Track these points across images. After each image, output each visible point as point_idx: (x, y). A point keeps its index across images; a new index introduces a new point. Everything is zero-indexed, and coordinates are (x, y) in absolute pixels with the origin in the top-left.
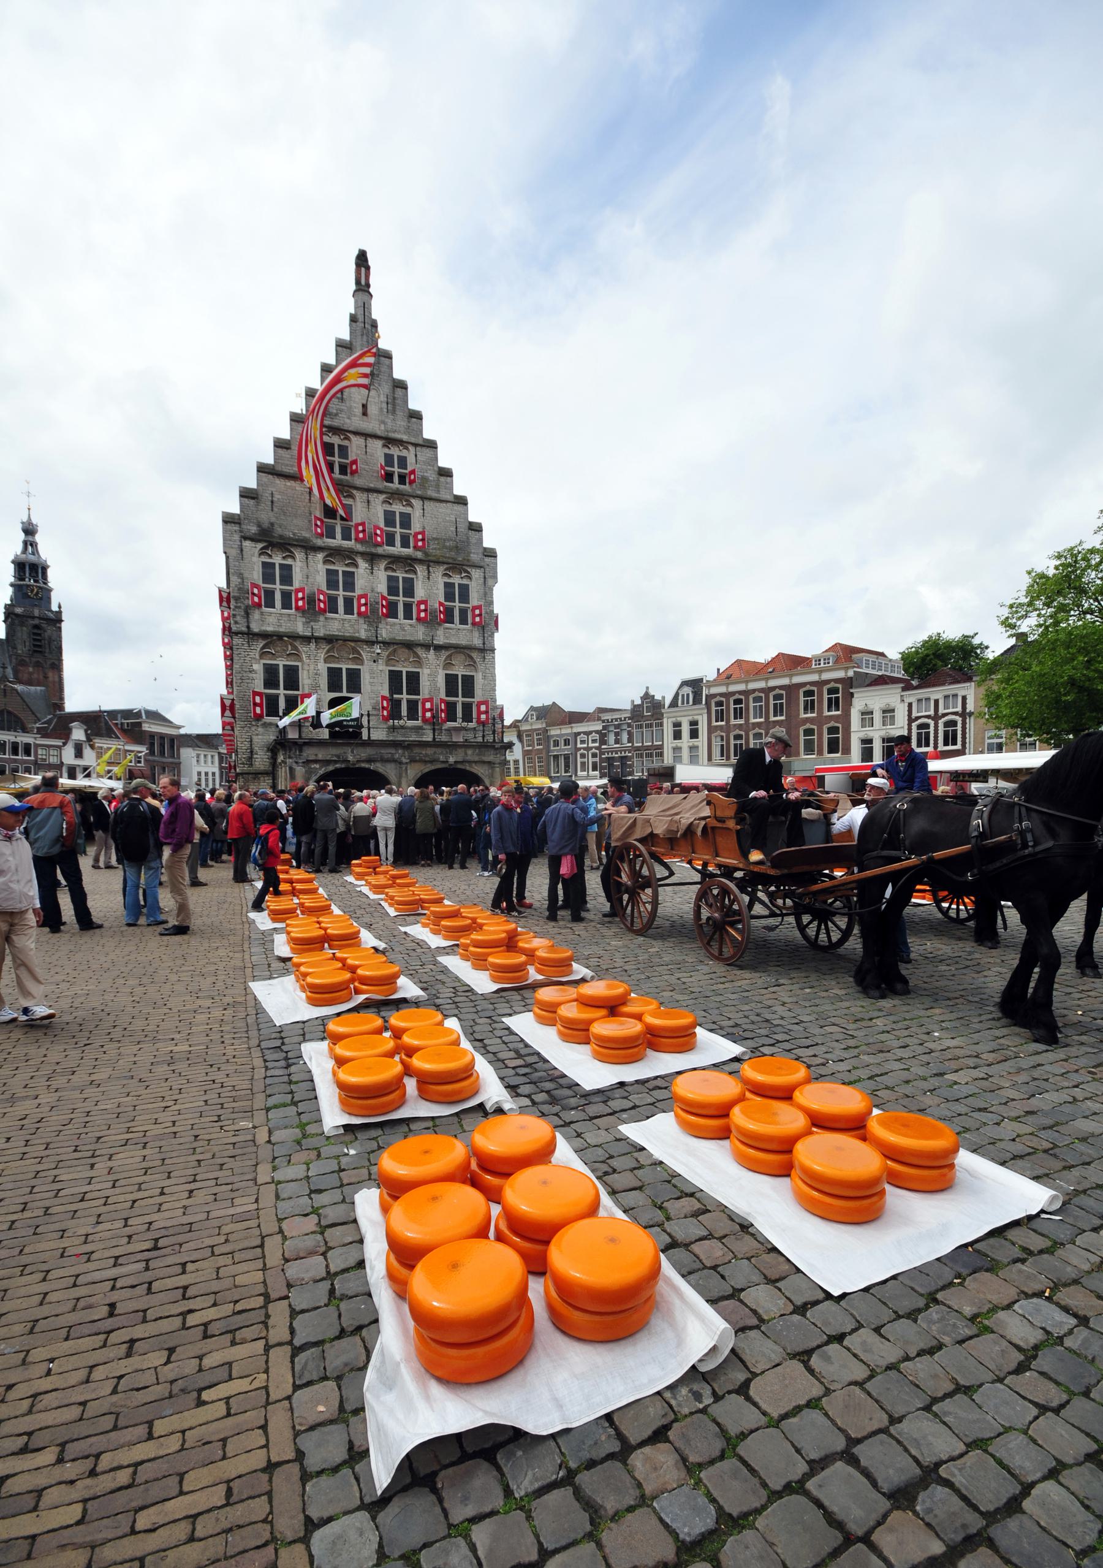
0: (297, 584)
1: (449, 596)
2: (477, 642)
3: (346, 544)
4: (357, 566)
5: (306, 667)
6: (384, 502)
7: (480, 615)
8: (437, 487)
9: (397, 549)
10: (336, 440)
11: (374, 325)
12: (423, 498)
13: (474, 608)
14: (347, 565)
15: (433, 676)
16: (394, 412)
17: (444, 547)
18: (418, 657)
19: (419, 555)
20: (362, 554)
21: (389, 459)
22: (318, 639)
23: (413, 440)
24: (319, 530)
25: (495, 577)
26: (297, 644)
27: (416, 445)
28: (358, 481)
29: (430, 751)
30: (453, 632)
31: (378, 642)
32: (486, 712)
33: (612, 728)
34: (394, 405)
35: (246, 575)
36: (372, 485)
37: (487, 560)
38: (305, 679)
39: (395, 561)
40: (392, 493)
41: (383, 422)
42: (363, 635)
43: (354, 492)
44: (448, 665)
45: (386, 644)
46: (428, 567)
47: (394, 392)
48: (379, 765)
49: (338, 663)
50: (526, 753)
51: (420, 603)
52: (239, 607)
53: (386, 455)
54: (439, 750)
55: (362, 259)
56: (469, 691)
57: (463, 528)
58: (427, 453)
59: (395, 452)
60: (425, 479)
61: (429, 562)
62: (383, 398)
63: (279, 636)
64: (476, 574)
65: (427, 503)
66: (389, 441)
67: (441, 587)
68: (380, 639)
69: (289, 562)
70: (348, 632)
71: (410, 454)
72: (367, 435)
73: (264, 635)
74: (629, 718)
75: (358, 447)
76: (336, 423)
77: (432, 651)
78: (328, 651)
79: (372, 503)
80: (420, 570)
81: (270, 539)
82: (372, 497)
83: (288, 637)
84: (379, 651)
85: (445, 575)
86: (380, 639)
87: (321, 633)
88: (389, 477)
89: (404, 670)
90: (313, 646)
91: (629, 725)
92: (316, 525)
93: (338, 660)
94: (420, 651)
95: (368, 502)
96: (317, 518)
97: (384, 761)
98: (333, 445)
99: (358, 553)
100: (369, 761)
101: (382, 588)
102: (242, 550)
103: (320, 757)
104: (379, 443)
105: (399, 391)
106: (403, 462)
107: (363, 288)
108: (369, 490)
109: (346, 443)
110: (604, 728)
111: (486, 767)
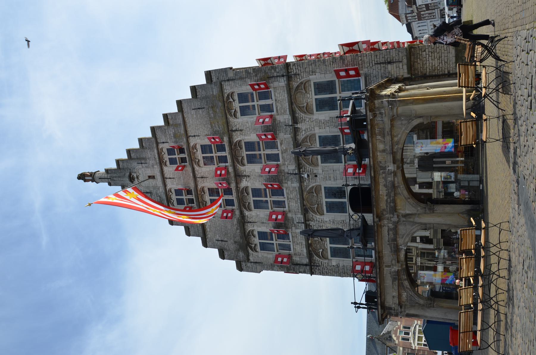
2: (282, 82)
4: (247, 188)
6: (199, 165)
7: (258, 85)
8: (176, 125)
12: (188, 137)
14: (248, 194)
15: (321, 124)
18: (306, 138)
19: (226, 139)
20: (237, 184)
21: (173, 162)
23: (155, 145)
27: (157, 144)
28: (192, 186)
32: (347, 71)
36: (191, 174)
37: (214, 79)
41: (153, 166)
42: (296, 185)
43: (199, 187)
44: (308, 110)
46: (232, 131)
47: (134, 159)
49: (322, 205)
52: (294, 268)
55: (82, 177)
57: (197, 104)
58: (158, 133)
59: (166, 157)
60: (175, 136)
61: (230, 132)
64: (228, 89)
67: (245, 118)
68: (297, 171)
70: (295, 195)
71: (165, 147)
72: (164, 179)
73: (310, 255)
75: (173, 184)
76: (164, 197)
77: (299, 126)
78: (314, 212)
79: (202, 174)
80: (237, 137)
82: (198, 175)
84: (306, 176)
86: (297, 171)
93: (319, 205)
94: (301, 136)
95: (202, 178)
102: (256, 263)
103: (395, 294)
104: (165, 169)
111: (397, 123)
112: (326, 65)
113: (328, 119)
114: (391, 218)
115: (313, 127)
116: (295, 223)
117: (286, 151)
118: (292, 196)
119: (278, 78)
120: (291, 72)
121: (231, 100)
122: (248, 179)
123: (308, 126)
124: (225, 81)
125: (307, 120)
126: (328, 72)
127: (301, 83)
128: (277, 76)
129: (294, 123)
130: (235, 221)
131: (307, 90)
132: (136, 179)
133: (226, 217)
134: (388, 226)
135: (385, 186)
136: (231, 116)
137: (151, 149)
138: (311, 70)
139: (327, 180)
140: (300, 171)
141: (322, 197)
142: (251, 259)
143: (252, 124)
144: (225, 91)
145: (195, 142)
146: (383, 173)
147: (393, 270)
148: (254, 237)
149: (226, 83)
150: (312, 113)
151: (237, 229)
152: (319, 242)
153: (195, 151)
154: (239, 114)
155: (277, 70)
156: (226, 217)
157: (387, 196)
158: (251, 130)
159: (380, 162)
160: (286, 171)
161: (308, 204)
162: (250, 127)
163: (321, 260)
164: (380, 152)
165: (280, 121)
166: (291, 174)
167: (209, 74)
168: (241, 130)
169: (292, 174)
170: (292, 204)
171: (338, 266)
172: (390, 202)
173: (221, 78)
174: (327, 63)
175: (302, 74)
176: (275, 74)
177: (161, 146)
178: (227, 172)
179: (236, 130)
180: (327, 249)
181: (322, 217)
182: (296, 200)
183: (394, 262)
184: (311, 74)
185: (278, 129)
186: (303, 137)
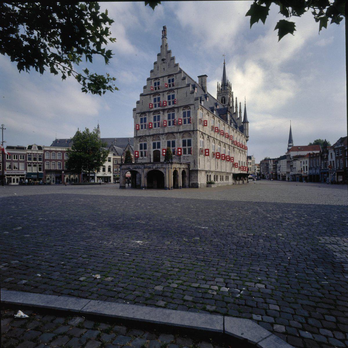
4: (160, 113)
6: (168, 93)
15: (178, 141)
20: (162, 110)
23: (175, 73)
26: (146, 137)
28: (161, 90)
29: (149, 165)
36: (165, 90)
37: (196, 101)
39: (170, 109)
44: (183, 137)
45: (166, 134)
48: (138, 169)
50: (336, 158)
55: (164, 28)
56: (190, 144)
63: (143, 136)
68: (165, 133)
73: (140, 137)
78: (153, 138)
87: (151, 134)
89: (171, 140)
93: (155, 140)
94: (175, 135)
97: (138, 168)
100: (135, 168)
103: (125, 168)
104: (167, 77)
107: (164, 36)
133: (150, 106)
142: (137, 115)
156: (150, 106)
171: (138, 146)
173: (196, 104)
177: (175, 75)
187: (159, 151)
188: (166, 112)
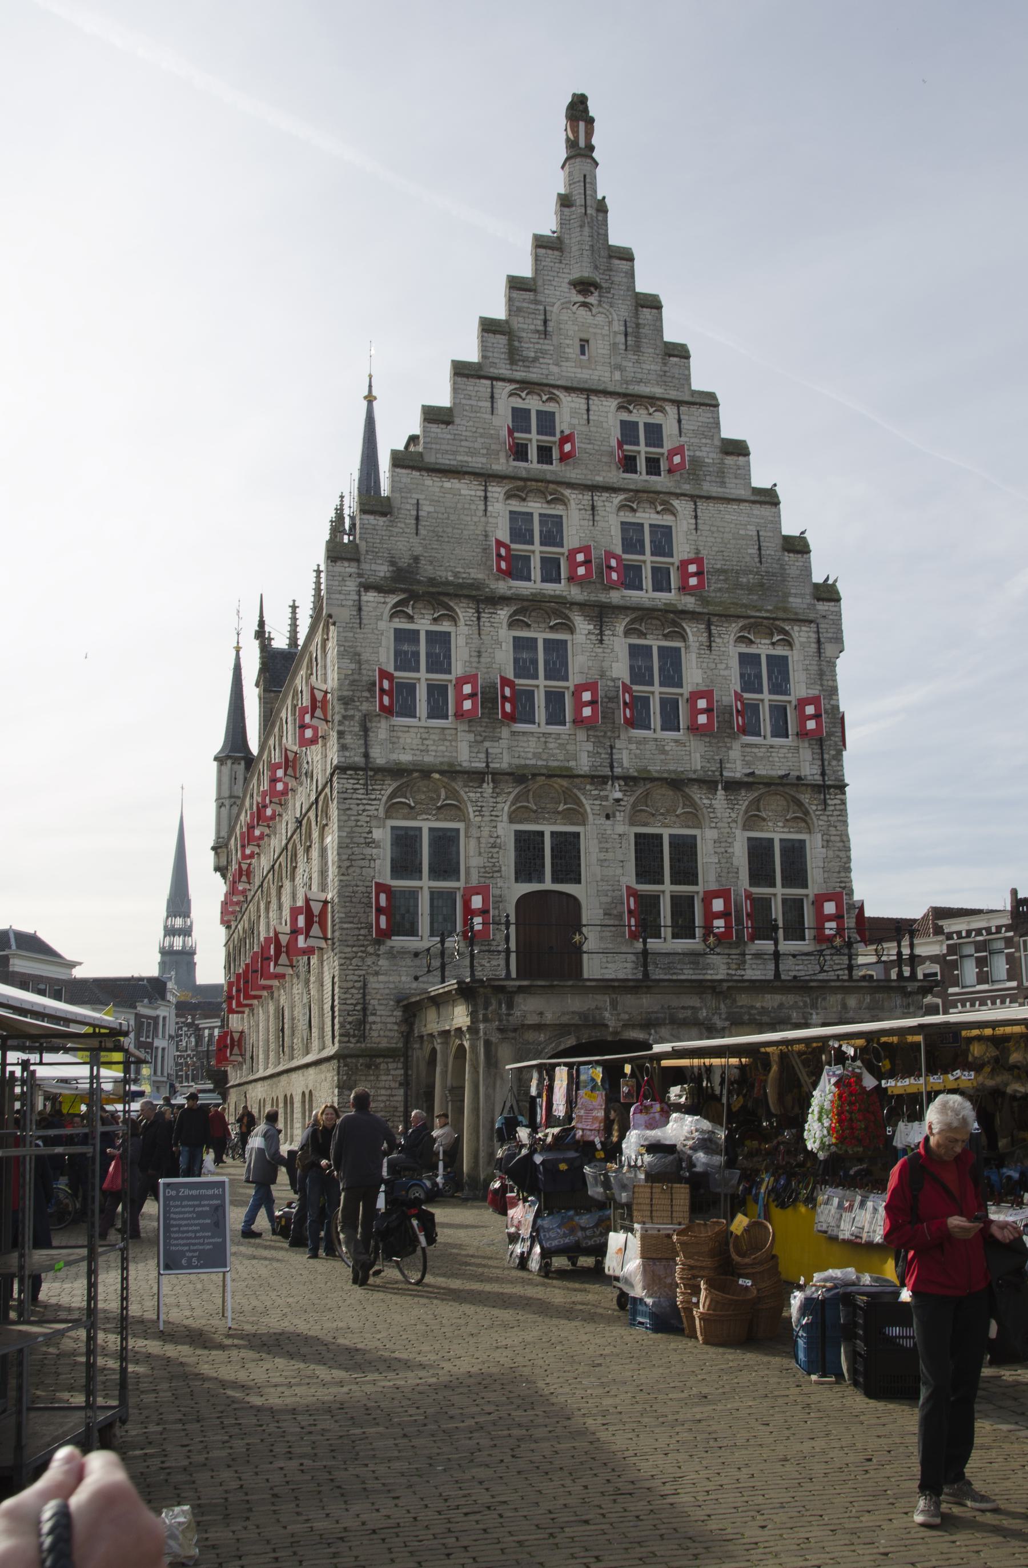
0: (458, 669)
1: (751, 683)
2: (809, 770)
3: (550, 588)
4: (571, 630)
5: (474, 832)
6: (621, 507)
8: (721, 475)
9: (646, 596)
10: (533, 404)
11: (602, 207)
12: (694, 498)
13: (802, 703)
14: (551, 628)
15: (724, 843)
16: (637, 349)
17: (738, 586)
18: (693, 804)
19: (689, 602)
21: (629, 430)
22: (497, 776)
23: (673, 394)
24: (503, 565)
25: (838, 640)
26: (458, 785)
27: (678, 403)
30: (760, 752)
31: (615, 778)
33: (970, 950)
34: (638, 336)
35: (364, 657)
36: (599, 479)
37: (822, 607)
38: (470, 856)
40: (637, 491)
41: (619, 367)
42: (584, 764)
43: (567, 492)
44: (752, 820)
45: (629, 781)
47: (636, 315)
49: (536, 821)
51: (695, 696)
53: (623, 423)
54: (790, 999)
55: (578, 110)
56: (796, 875)
57: (772, 548)
59: (640, 416)
60: (697, 463)
62: (618, 327)
63: (426, 772)
64: (801, 635)
65: (702, 505)
66: (629, 400)
67: (734, 663)
68: (618, 771)
69: (445, 627)
71: (668, 421)
72: (589, 392)
73: (397, 771)
74: (1009, 927)
75: (574, 413)
76: (534, 375)
77: (720, 793)
79: (600, 512)
80: (694, 632)
81: (413, 587)
82: (600, 498)
83: (442, 773)
84: (618, 795)
85: (741, 639)
86: (618, 771)
87: (504, 762)
88: (629, 464)
90: (488, 788)
91: (1009, 942)
92: (499, 555)
93: (536, 816)
94: (698, 795)
95: (593, 508)
96: (499, 544)
98: (528, 411)
99: (572, 604)
101: (620, 669)
102: (360, 609)
103: (549, 1018)
104: (612, 403)
105: (646, 314)
106: (655, 434)
108: (594, 488)
109: (550, 407)
110: (952, 949)
112: (839, 872)
113: (736, 862)
114: (720, 1014)
115: (719, 825)
116: (487, 744)
117: (664, 752)
118: (551, 746)
119: (820, 763)
120: (830, 794)
121: (776, 638)
122: (593, 637)
123: (719, 815)
124: (818, 632)
125: (734, 815)
126: (826, 875)
127: (806, 813)
128: (823, 760)
129: (726, 782)
130: (477, 574)
131: (790, 824)
132: (580, 298)
134: (701, 1009)
135: (781, 1006)
136: (742, 629)
137: (663, 378)
138: (832, 838)
139: (600, 842)
140: (618, 778)
141: (555, 823)
142: (370, 597)
143: (725, 677)
144: (796, 628)
145: (680, 516)
146: (805, 1002)
147: (607, 1015)
148: (435, 620)
149: (814, 636)
150: (746, 828)
151: (456, 575)
152: (432, 799)
153: (659, 508)
154: (744, 649)
155: (834, 763)
157: (762, 1007)
158: (709, 673)
159: (824, 999)
160: (618, 744)
161: (536, 786)
162: (716, 672)
163: (384, 798)
164: (843, 999)
165: (730, 748)
166: (611, 754)
167: (828, 593)
168: (710, 647)
169: (612, 759)
170: (532, 744)
171: (370, 843)
172: (750, 1014)
174: (843, 874)
175: (825, 818)
176: (826, 756)
177: (671, 410)
178: (612, 586)
179: (710, 635)
180: (415, 819)
181: (505, 818)
182: (545, 757)
183: (627, 1017)
184: (825, 837)
185: (714, 741)
186: (696, 797)
187: (573, 903)
188: (620, 628)
